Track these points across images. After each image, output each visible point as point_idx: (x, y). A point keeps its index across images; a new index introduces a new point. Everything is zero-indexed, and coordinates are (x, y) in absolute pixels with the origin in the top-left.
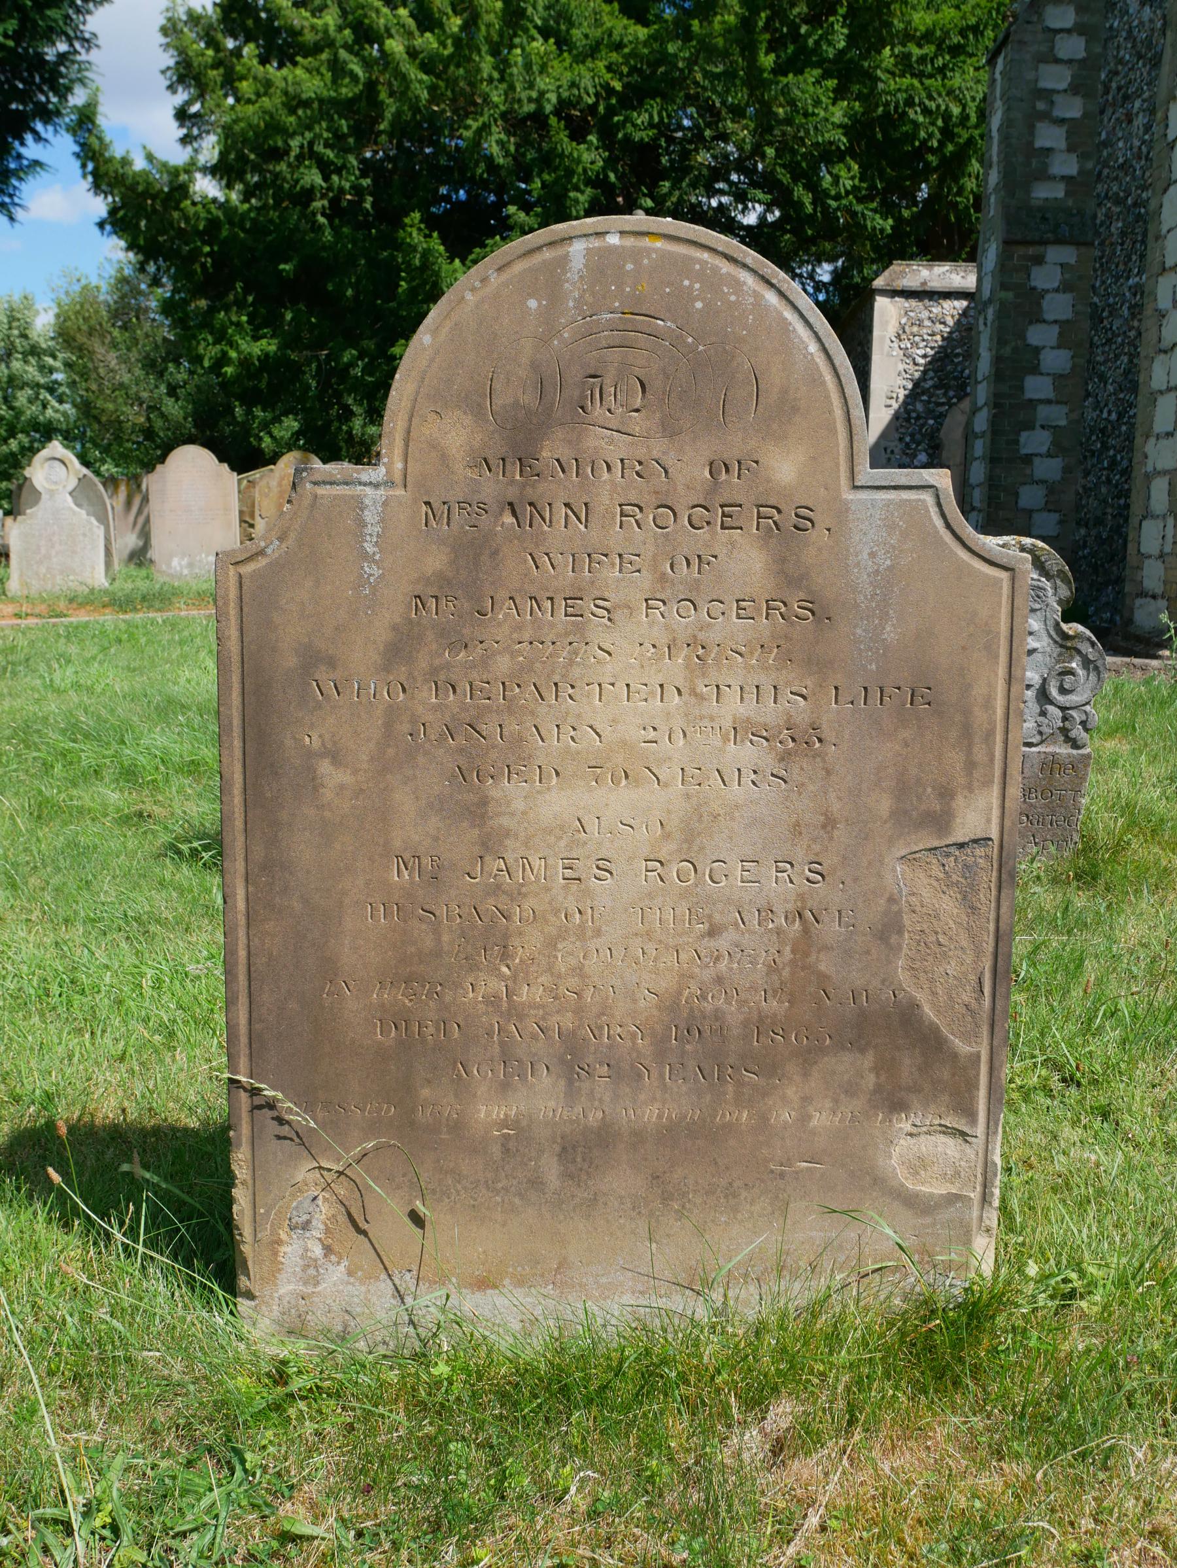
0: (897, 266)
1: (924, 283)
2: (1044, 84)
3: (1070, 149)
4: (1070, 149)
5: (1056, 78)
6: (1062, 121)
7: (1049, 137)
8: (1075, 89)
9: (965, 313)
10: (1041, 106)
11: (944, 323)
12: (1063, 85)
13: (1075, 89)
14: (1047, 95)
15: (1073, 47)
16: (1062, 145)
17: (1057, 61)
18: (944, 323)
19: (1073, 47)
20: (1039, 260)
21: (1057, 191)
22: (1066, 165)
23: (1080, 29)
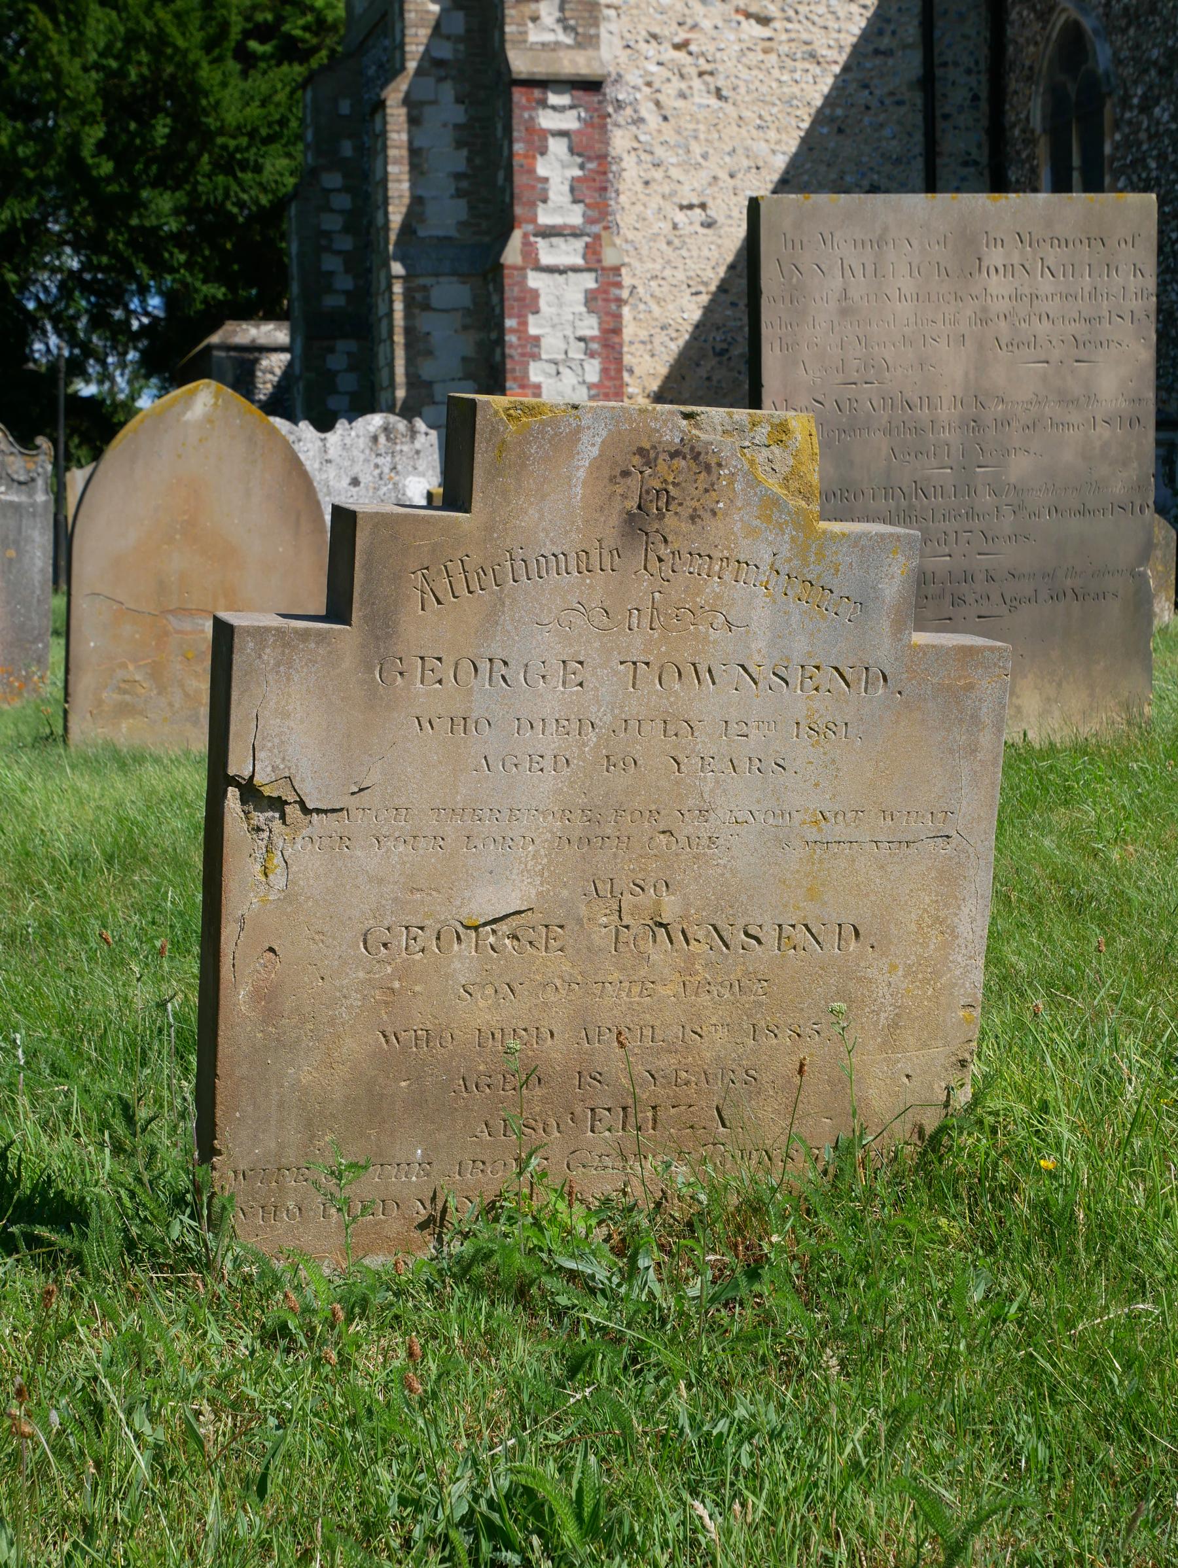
0: (229, 326)
1: (253, 341)
2: (325, 227)
3: (347, 272)
4: (347, 272)
5: (331, 222)
6: (339, 253)
7: (331, 263)
8: (347, 229)
9: (290, 365)
10: (324, 242)
11: (272, 373)
12: (338, 227)
13: (347, 229)
14: (328, 234)
15: (343, 201)
16: (341, 269)
17: (332, 211)
18: (272, 373)
19: (343, 201)
20: (332, 350)
21: (341, 301)
22: (345, 282)
23: (346, 189)
